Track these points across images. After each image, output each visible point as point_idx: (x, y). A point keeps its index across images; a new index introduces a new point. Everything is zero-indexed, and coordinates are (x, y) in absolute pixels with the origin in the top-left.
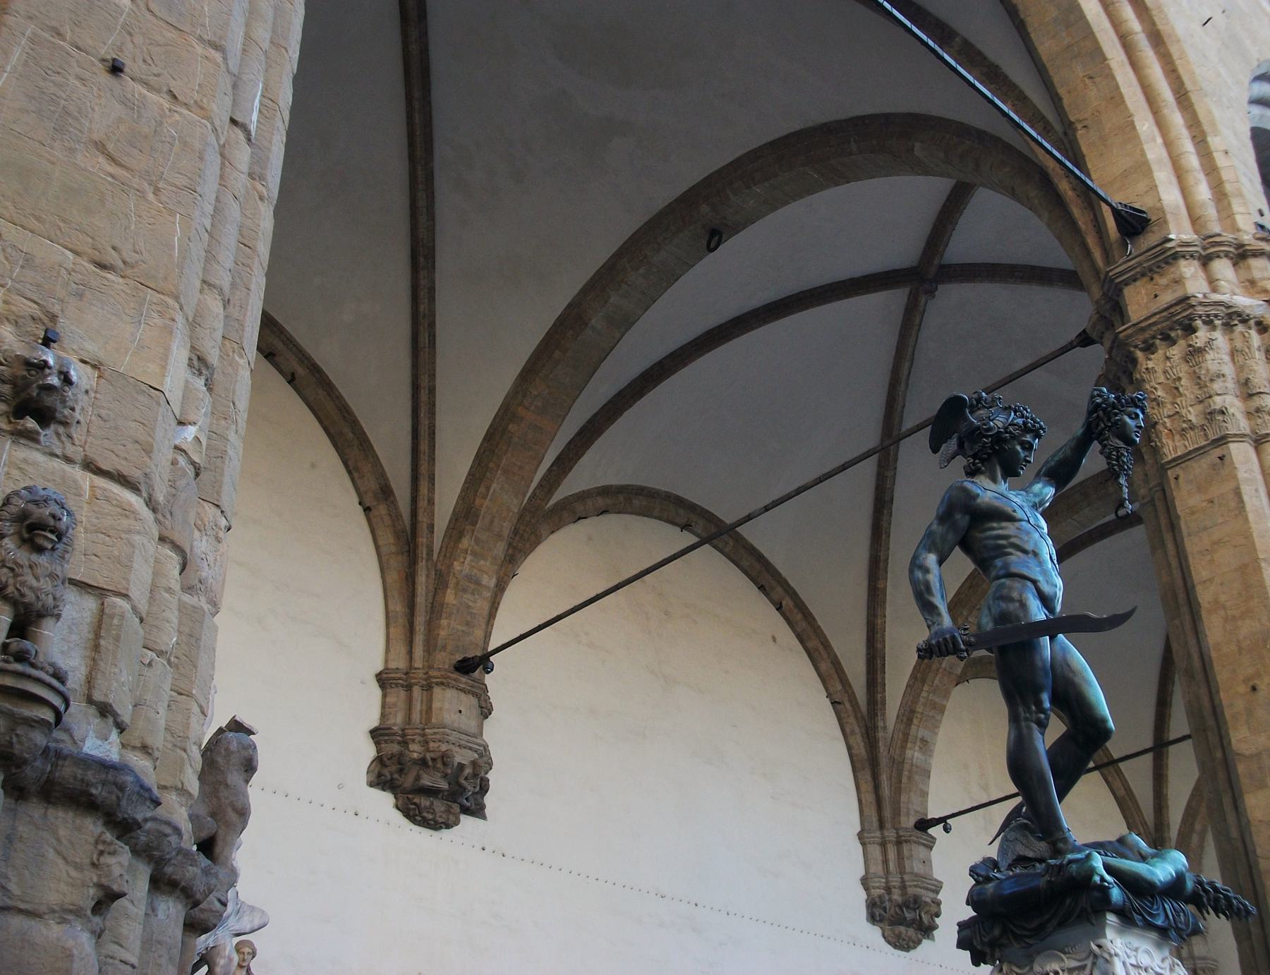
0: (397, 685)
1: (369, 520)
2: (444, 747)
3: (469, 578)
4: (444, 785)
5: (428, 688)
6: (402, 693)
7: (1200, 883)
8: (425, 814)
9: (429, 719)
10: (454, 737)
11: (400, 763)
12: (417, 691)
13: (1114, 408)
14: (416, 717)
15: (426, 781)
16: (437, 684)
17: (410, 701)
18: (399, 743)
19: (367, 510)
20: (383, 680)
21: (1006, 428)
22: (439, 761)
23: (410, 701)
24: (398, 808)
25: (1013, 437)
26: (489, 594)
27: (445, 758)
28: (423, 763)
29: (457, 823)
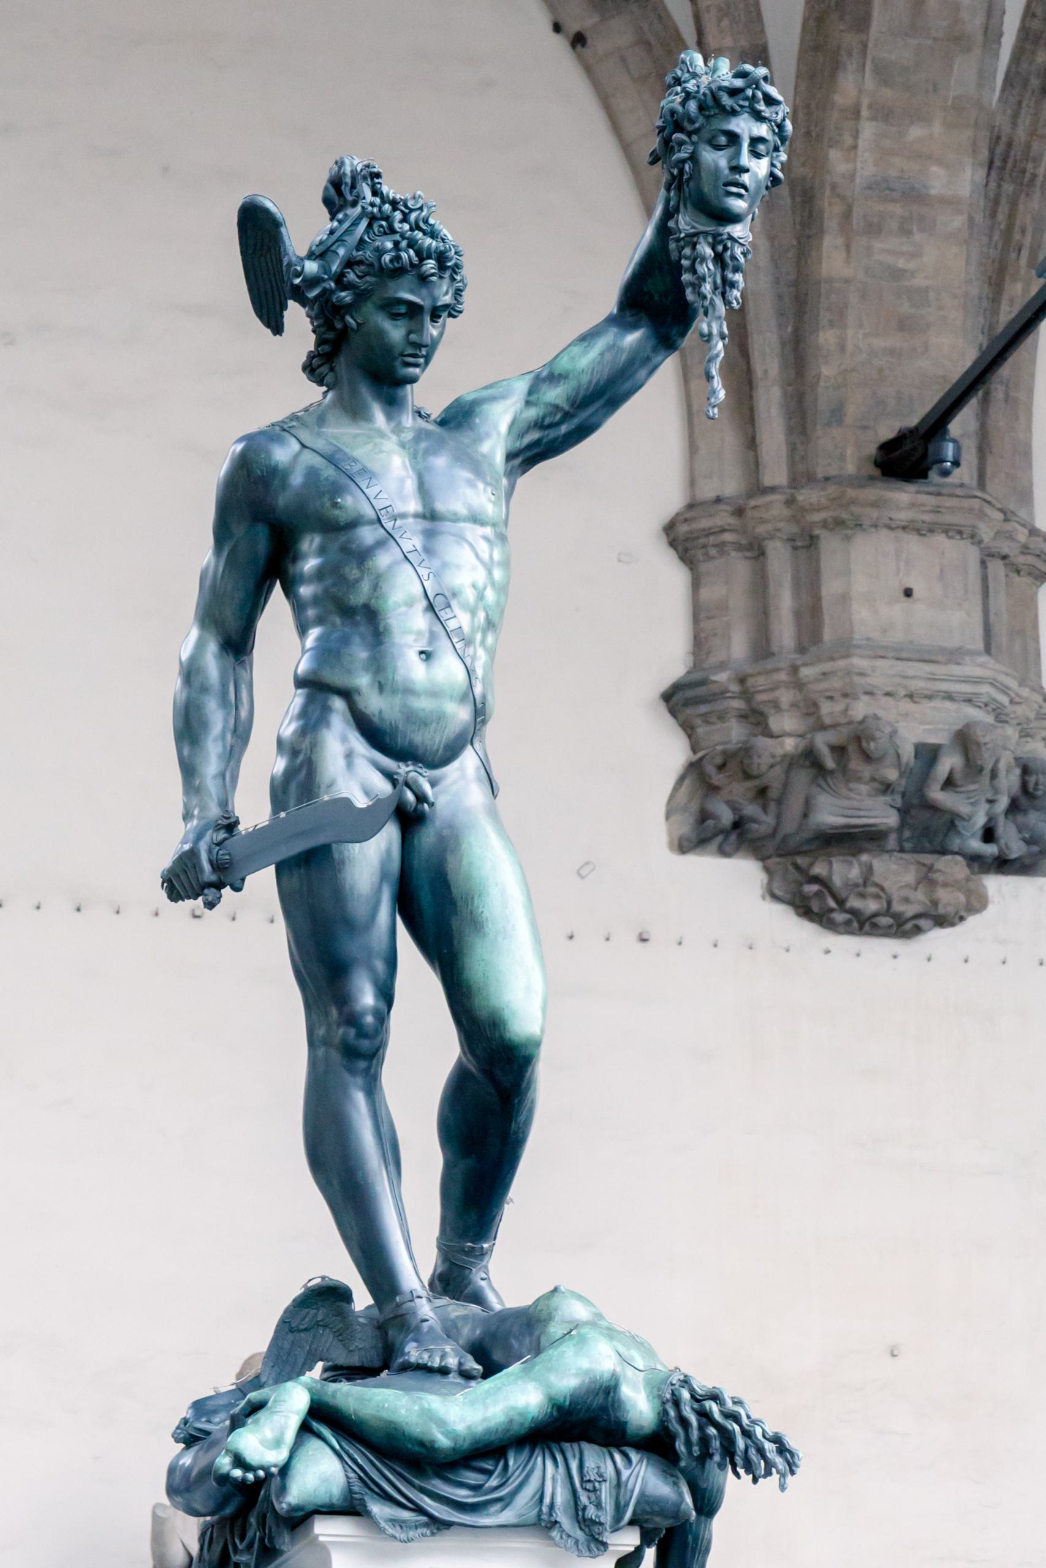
0: (721, 546)
1: (588, 69)
2: (860, 709)
3: (882, 188)
4: (883, 814)
5: (806, 544)
6: (740, 568)
7: (677, 1403)
8: (854, 903)
9: (816, 637)
10: (882, 673)
11: (748, 776)
12: (780, 559)
13: (678, 127)
14: (785, 633)
15: (830, 813)
16: (825, 524)
17: (760, 588)
18: (743, 717)
19: (578, 40)
20: (684, 539)
21: (339, 278)
22: (852, 749)
23: (760, 588)
24: (775, 897)
25: (362, 296)
26: (958, 222)
27: (856, 746)
28: (809, 758)
29: (976, 903)
